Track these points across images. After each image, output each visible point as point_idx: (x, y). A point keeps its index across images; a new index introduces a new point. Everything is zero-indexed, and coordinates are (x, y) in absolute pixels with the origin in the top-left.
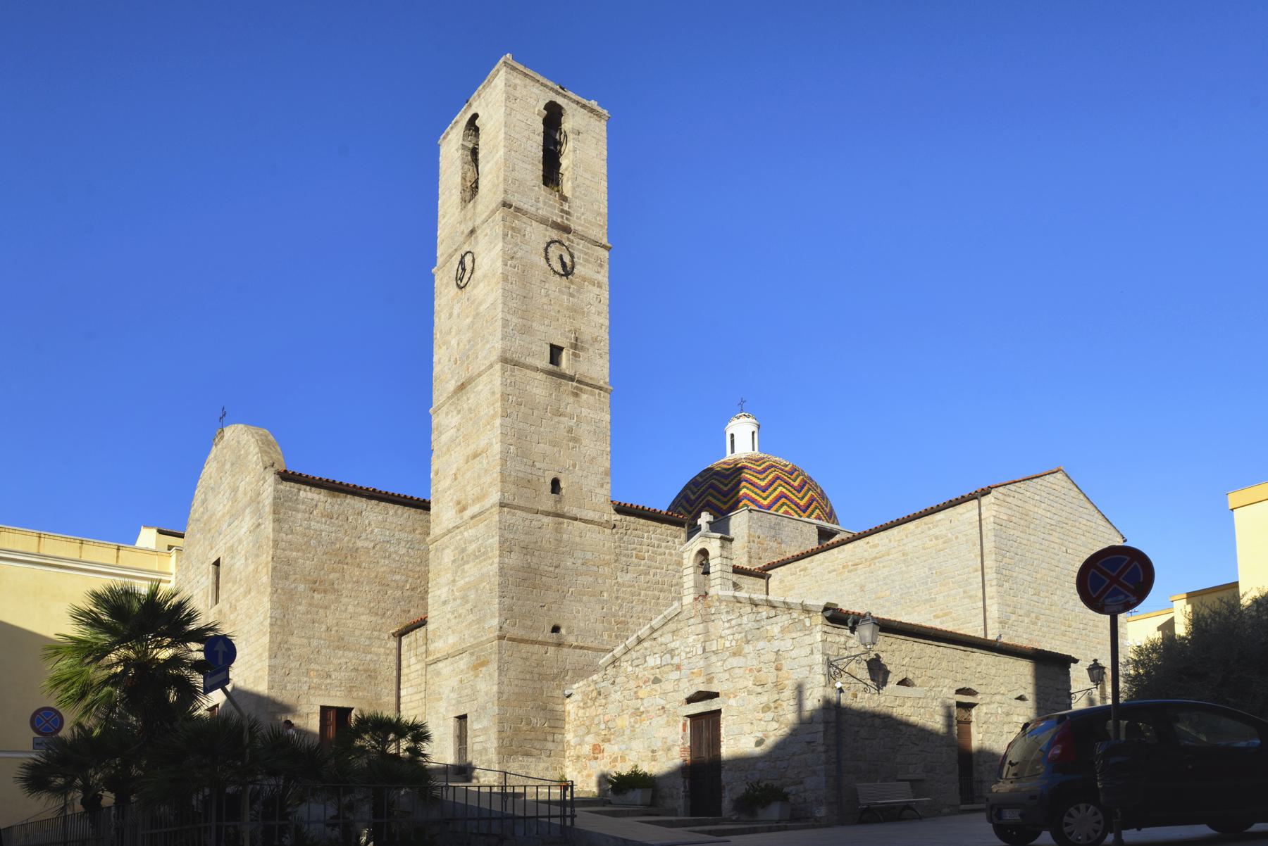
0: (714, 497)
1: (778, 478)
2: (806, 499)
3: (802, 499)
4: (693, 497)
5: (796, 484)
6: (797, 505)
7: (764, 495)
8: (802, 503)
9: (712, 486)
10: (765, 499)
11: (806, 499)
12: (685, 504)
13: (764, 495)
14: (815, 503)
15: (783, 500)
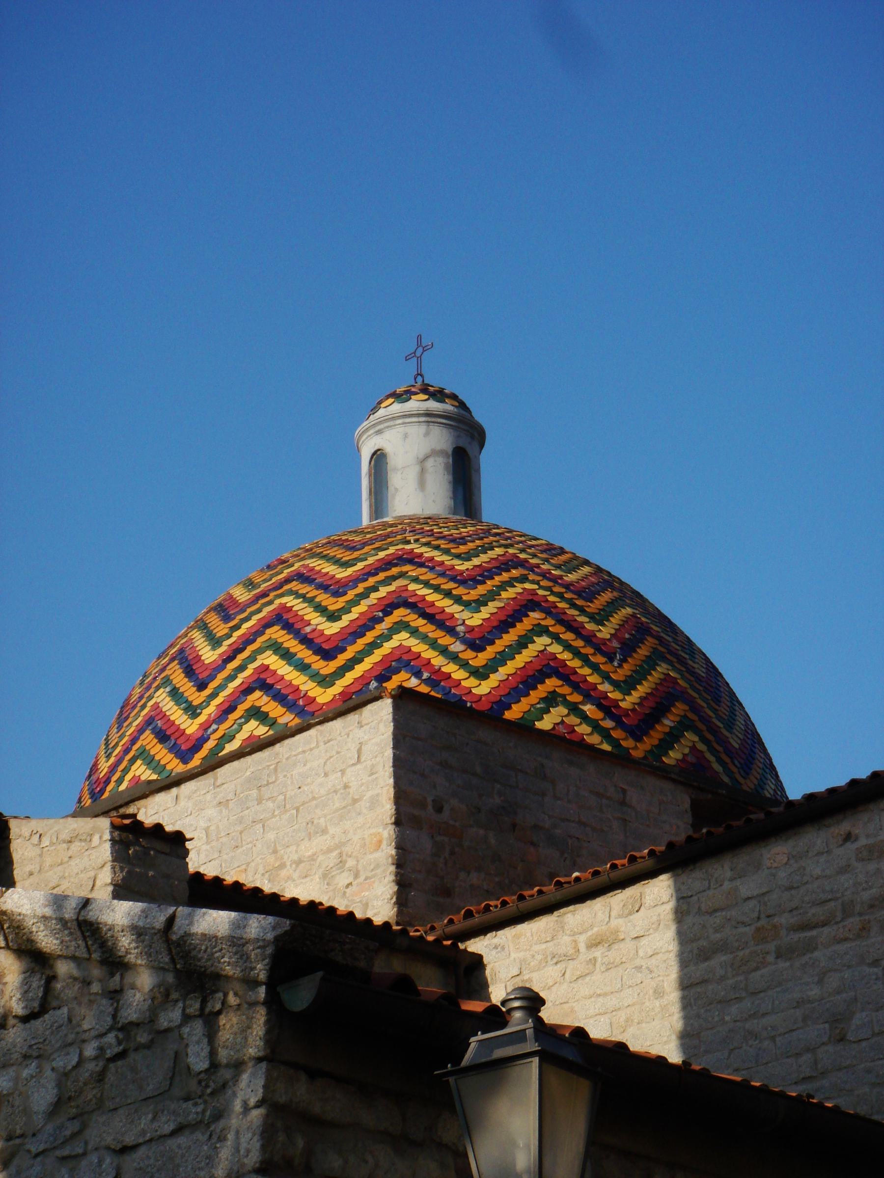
0: (286, 655)
1: (530, 603)
2: (642, 689)
3: (627, 686)
4: (209, 655)
5: (605, 632)
6: (607, 707)
7: (480, 659)
8: (628, 702)
9: (284, 619)
10: (481, 674)
11: (642, 689)
12: (179, 678)
13: (480, 659)
14: (679, 708)
15: (552, 683)
